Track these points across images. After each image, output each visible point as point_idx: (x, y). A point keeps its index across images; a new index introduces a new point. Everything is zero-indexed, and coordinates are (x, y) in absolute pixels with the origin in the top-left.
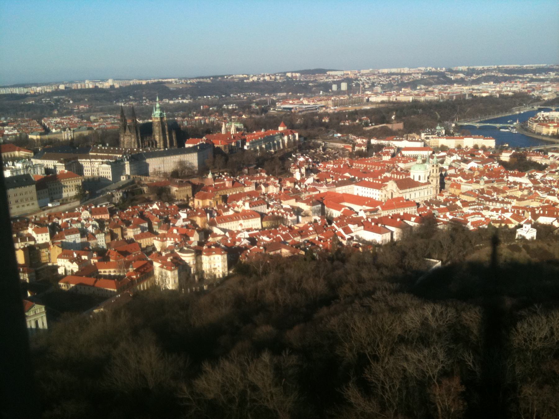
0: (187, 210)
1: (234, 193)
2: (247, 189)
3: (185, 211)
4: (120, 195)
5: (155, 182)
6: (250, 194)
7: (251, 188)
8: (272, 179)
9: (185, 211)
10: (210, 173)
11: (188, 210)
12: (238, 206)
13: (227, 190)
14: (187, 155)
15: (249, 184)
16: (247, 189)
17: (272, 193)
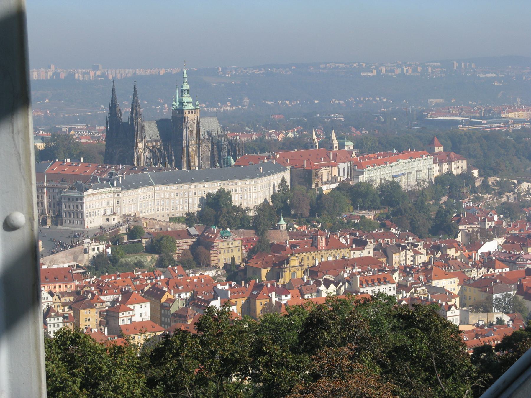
0: (230, 286)
1: (330, 259)
2: (357, 254)
3: (227, 287)
4: (98, 249)
5: (169, 229)
6: (363, 262)
7: (368, 252)
8: (410, 239)
9: (227, 287)
10: (282, 219)
11: (234, 284)
12: (336, 285)
13: (313, 254)
14: (238, 182)
15: (361, 244)
16: (357, 254)
17: (411, 268)
